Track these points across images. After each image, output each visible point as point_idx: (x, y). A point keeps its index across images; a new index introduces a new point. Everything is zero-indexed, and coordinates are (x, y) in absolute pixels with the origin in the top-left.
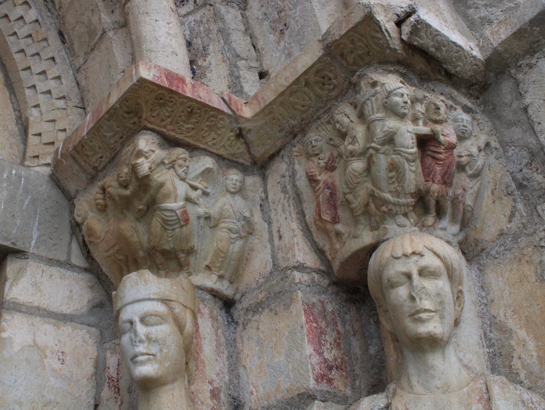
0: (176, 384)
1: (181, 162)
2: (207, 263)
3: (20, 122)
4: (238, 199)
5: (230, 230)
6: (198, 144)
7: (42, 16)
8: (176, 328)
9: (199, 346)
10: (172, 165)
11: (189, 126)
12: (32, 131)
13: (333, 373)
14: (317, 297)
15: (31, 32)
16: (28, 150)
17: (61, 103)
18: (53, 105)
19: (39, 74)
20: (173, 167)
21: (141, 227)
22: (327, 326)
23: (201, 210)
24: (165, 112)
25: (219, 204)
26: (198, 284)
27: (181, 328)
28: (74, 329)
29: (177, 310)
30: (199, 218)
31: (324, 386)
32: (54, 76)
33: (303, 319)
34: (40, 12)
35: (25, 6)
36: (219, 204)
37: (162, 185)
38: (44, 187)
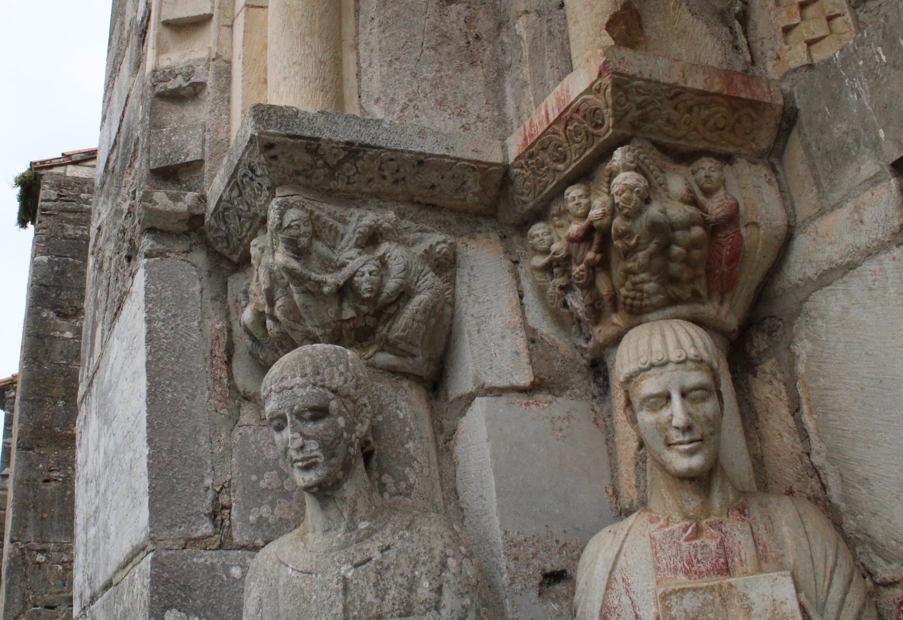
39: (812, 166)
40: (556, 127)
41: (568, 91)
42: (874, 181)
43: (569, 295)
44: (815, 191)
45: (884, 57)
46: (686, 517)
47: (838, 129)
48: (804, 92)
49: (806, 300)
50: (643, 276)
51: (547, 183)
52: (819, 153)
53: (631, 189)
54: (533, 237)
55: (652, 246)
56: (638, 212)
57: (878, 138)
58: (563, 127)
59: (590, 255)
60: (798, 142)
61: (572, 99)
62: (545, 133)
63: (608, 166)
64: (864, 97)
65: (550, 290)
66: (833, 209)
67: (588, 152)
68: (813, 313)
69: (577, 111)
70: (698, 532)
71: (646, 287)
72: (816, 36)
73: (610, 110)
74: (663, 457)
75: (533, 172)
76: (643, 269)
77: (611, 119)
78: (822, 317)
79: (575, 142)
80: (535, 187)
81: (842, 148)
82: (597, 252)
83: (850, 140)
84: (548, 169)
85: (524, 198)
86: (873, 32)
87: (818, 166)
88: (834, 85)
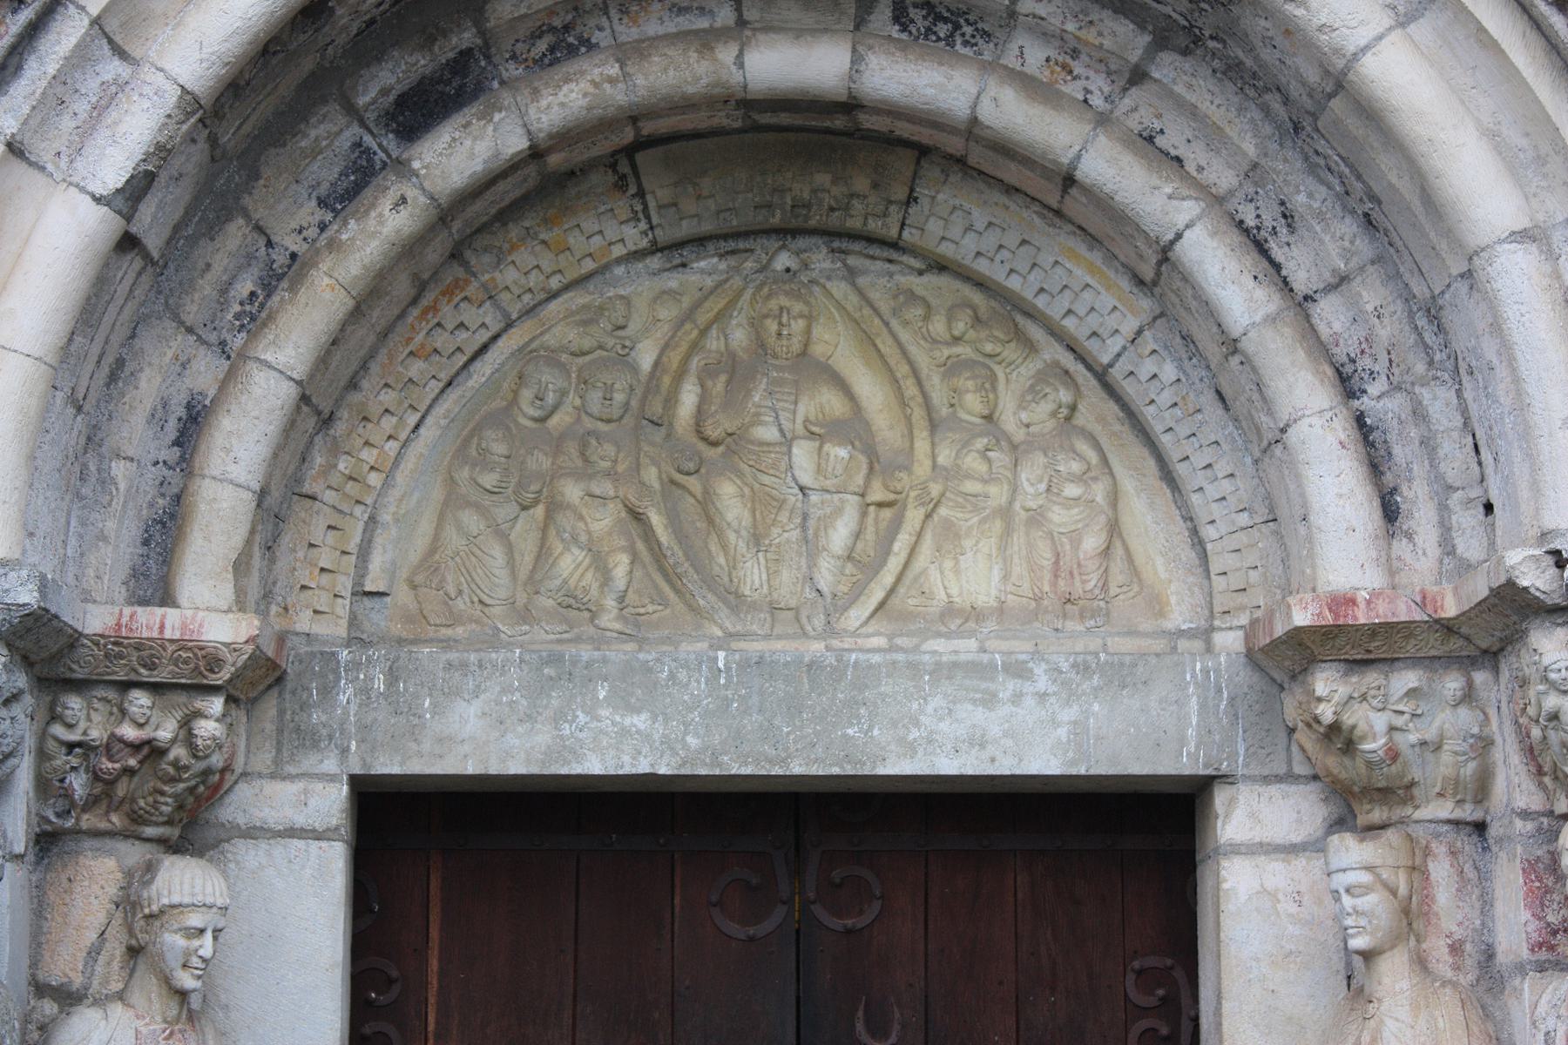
0: (1395, 951)
1: (1372, 692)
2: (1437, 790)
3: (1196, 540)
4: (1464, 713)
5: (1456, 753)
6: (1396, 656)
7: (1184, 372)
8: (1387, 894)
9: (1428, 899)
10: (1364, 698)
11: (1377, 644)
12: (1215, 567)
13: (1559, 937)
14: (1545, 848)
15: (1176, 399)
16: (1215, 602)
17: (1244, 519)
18: (1233, 522)
19: (1205, 468)
20: (1365, 699)
21: (1347, 761)
22: (1556, 883)
23: (1413, 738)
24: (1338, 642)
25: (1437, 723)
26: (1429, 817)
27: (1394, 893)
28: (1309, 859)
29: (1384, 876)
30: (1413, 746)
31: (1543, 955)
32: (1226, 473)
33: (1521, 881)
34: (1180, 368)
35: (1154, 356)
36: (1437, 723)
37: (1354, 727)
38: (1242, 674)
39: (280, 731)
40: (167, 644)
41: (201, 626)
42: (332, 778)
43: (73, 775)
44: (274, 754)
45: (382, 686)
46: (165, 1021)
47: (316, 717)
48: (301, 662)
49: (228, 841)
50: (169, 800)
51: (115, 673)
52: (292, 725)
53: (214, 738)
54: (67, 708)
55: (193, 783)
56: (207, 757)
57: (348, 746)
58: (174, 647)
59: (132, 762)
60: (275, 702)
61: (203, 638)
62: (148, 639)
63: (199, 704)
64: (352, 705)
65: (58, 762)
66: (284, 779)
67: (183, 681)
68: (229, 855)
69: (201, 649)
70: (171, 1034)
71: (164, 808)
72: (321, 609)
73: (233, 669)
74: (174, 973)
75: (107, 656)
76: (175, 796)
77: (228, 675)
78: (238, 863)
79: (177, 666)
80: (97, 667)
81: (314, 734)
82: (140, 762)
83: (324, 732)
84: (126, 665)
85: (75, 667)
86: (382, 659)
87: (286, 733)
88: (331, 677)
